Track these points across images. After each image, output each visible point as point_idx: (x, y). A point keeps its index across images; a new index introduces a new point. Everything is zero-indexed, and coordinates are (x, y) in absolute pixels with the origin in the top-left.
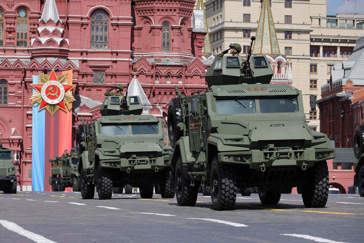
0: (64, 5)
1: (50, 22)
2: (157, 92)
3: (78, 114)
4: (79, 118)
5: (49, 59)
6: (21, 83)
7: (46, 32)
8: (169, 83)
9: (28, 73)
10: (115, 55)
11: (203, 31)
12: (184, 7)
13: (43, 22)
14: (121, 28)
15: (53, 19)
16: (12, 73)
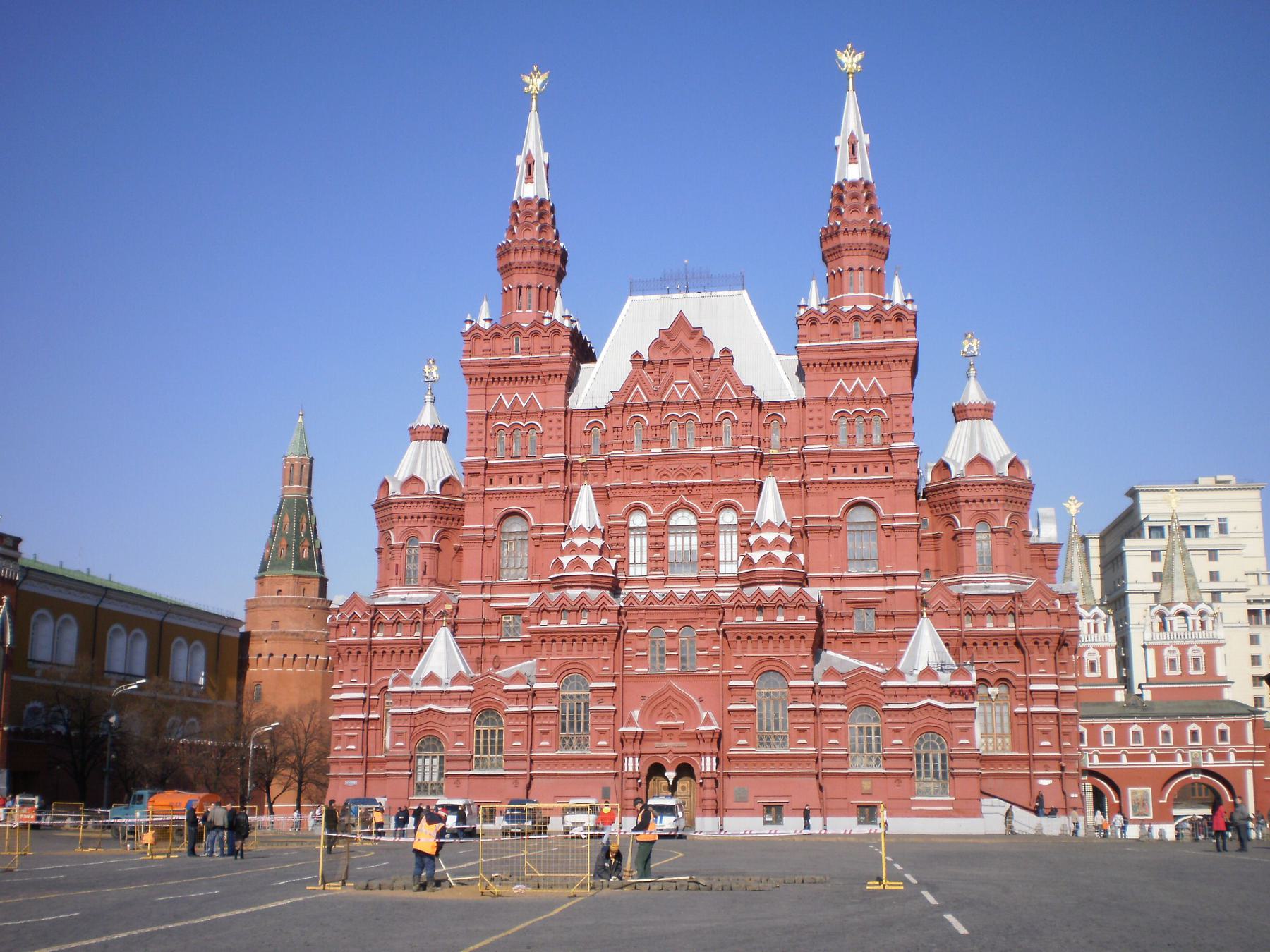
0: (797, 502)
1: (769, 525)
2: (969, 642)
3: (821, 684)
4: (823, 692)
5: (764, 588)
6: (718, 632)
7: (762, 543)
8: (990, 626)
9: (728, 612)
10: (890, 580)
11: (1055, 541)
12: (1013, 494)
13: (757, 528)
14: (899, 534)
15: (773, 520)
16: (701, 615)
